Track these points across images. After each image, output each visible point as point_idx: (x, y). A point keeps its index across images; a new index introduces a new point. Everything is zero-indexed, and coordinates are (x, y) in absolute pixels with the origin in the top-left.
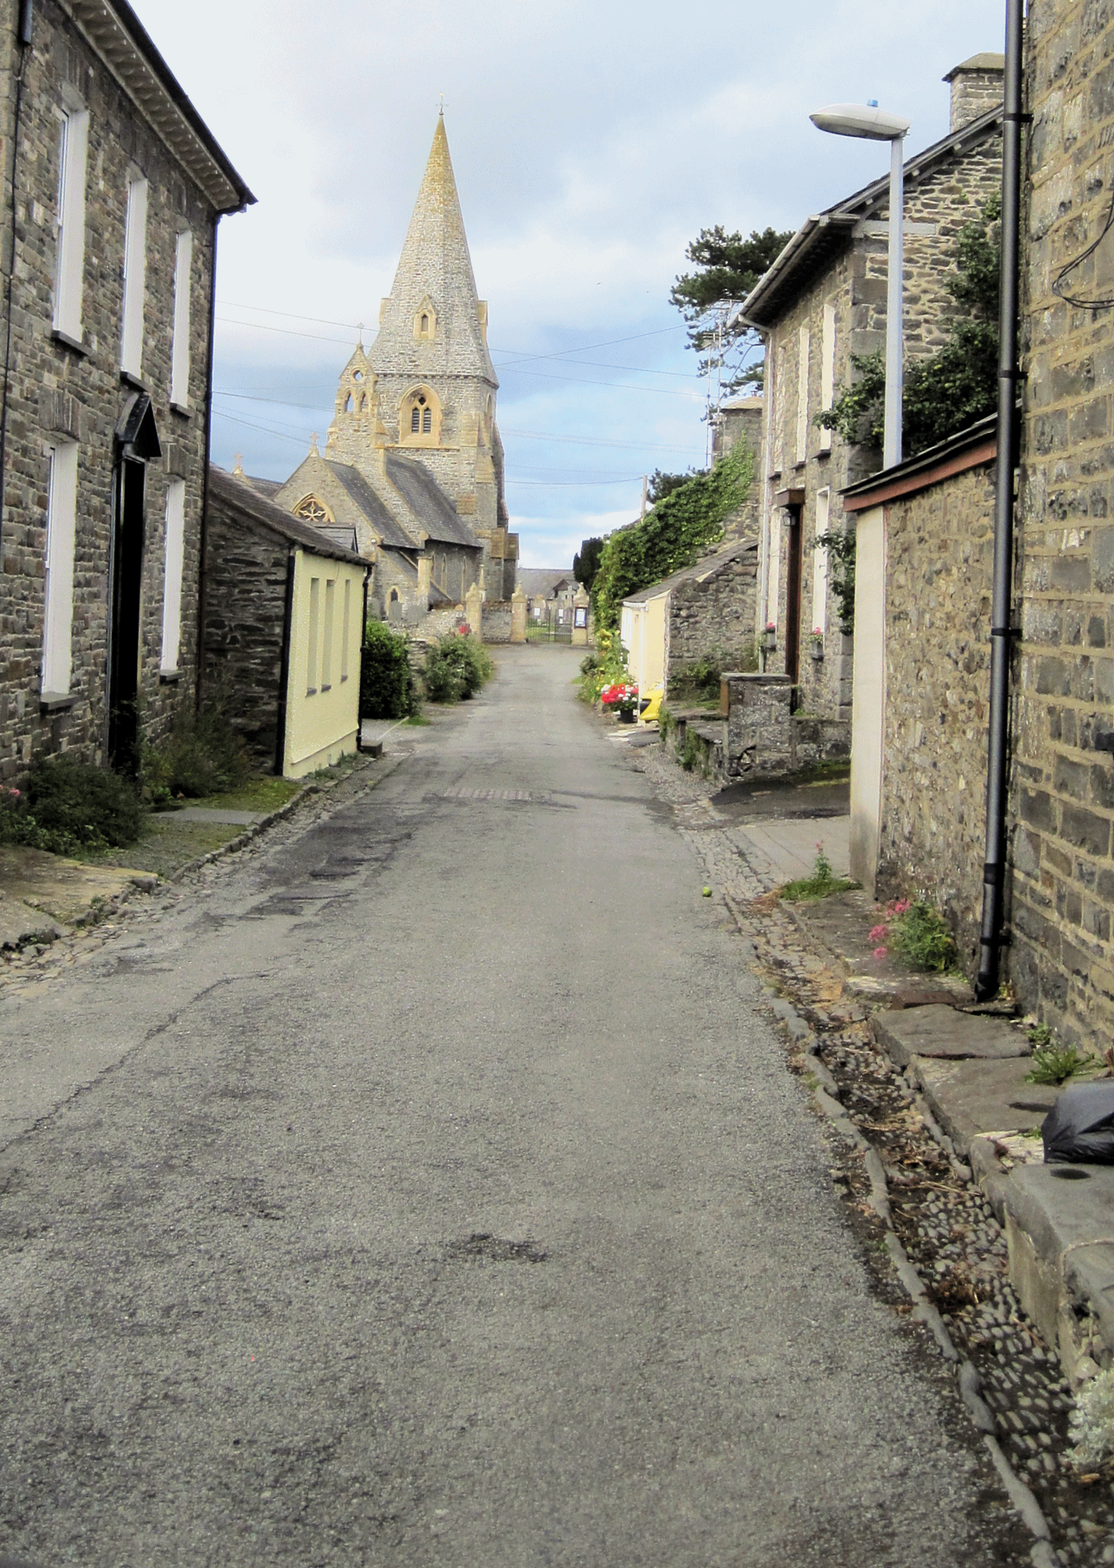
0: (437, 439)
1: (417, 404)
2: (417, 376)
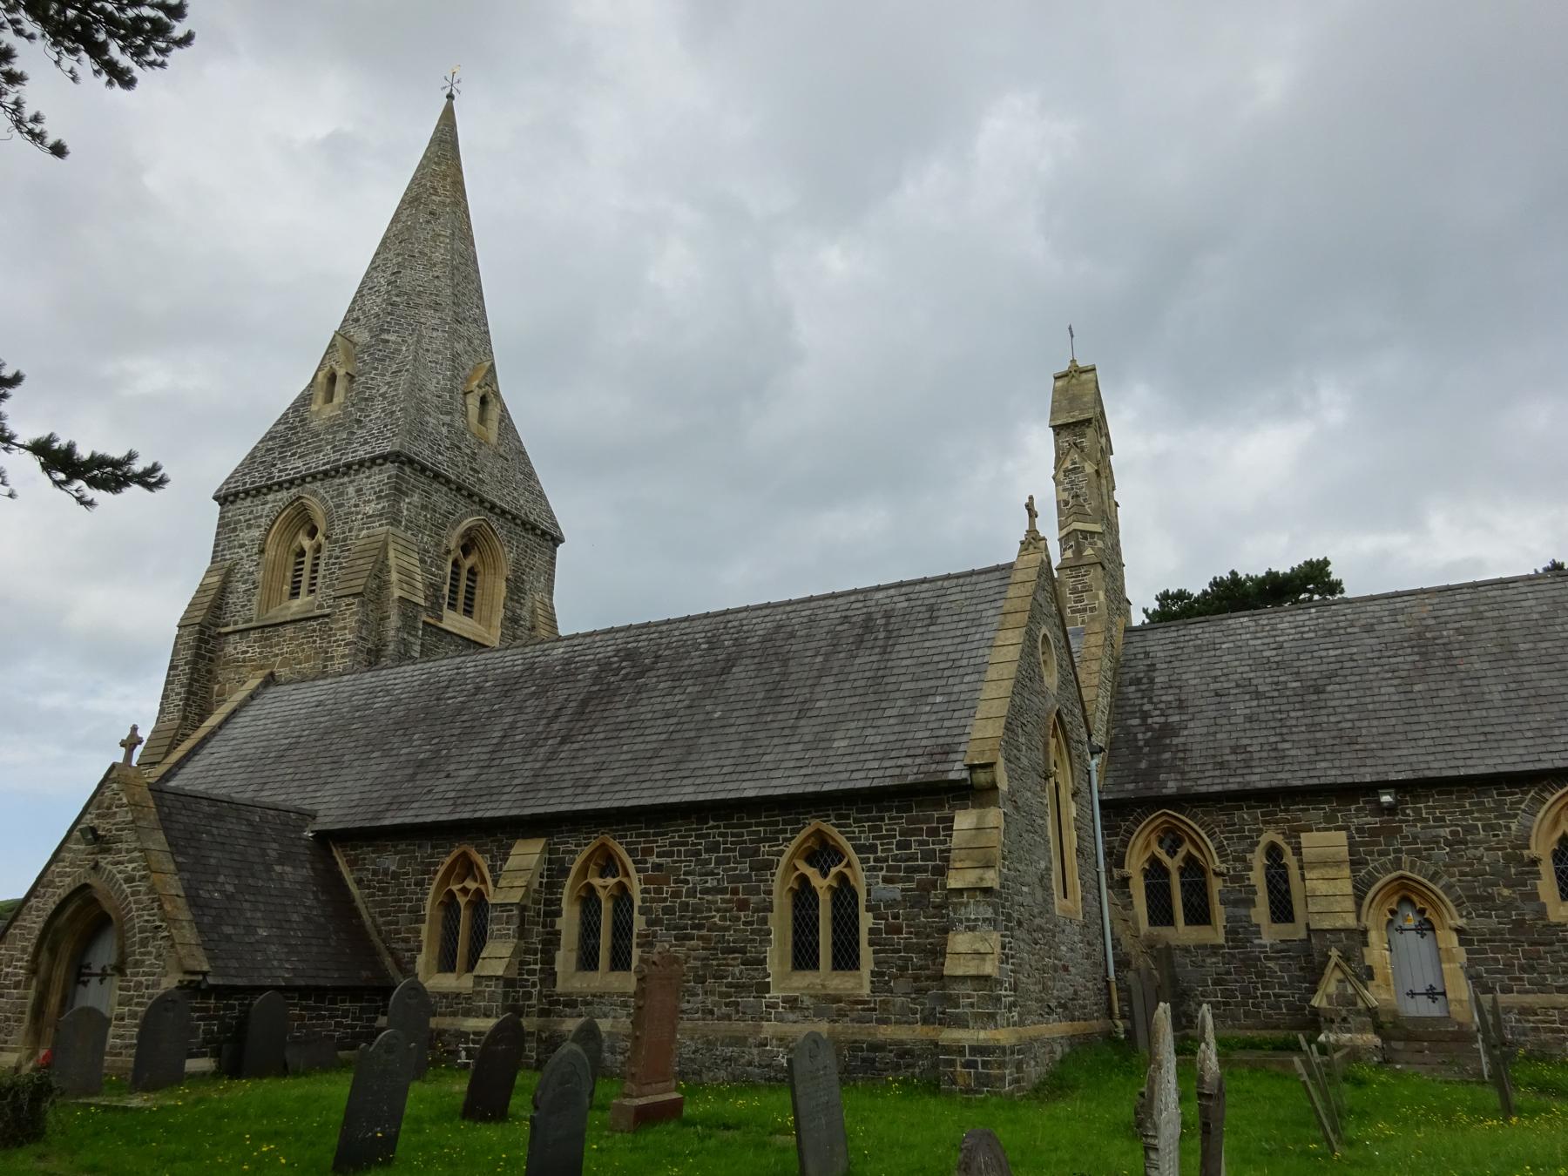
2: (482, 501)
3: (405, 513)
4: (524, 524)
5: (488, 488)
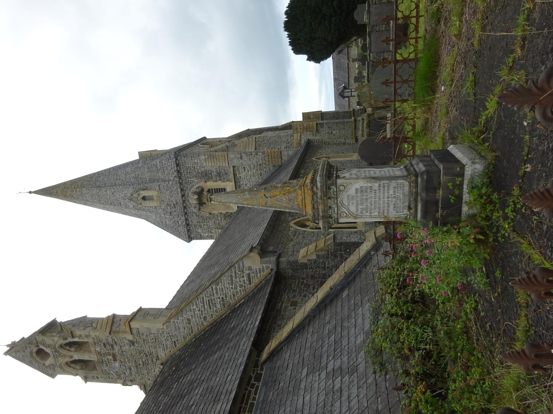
0: (228, 183)
2: (184, 202)
3: (207, 234)
5: (177, 199)
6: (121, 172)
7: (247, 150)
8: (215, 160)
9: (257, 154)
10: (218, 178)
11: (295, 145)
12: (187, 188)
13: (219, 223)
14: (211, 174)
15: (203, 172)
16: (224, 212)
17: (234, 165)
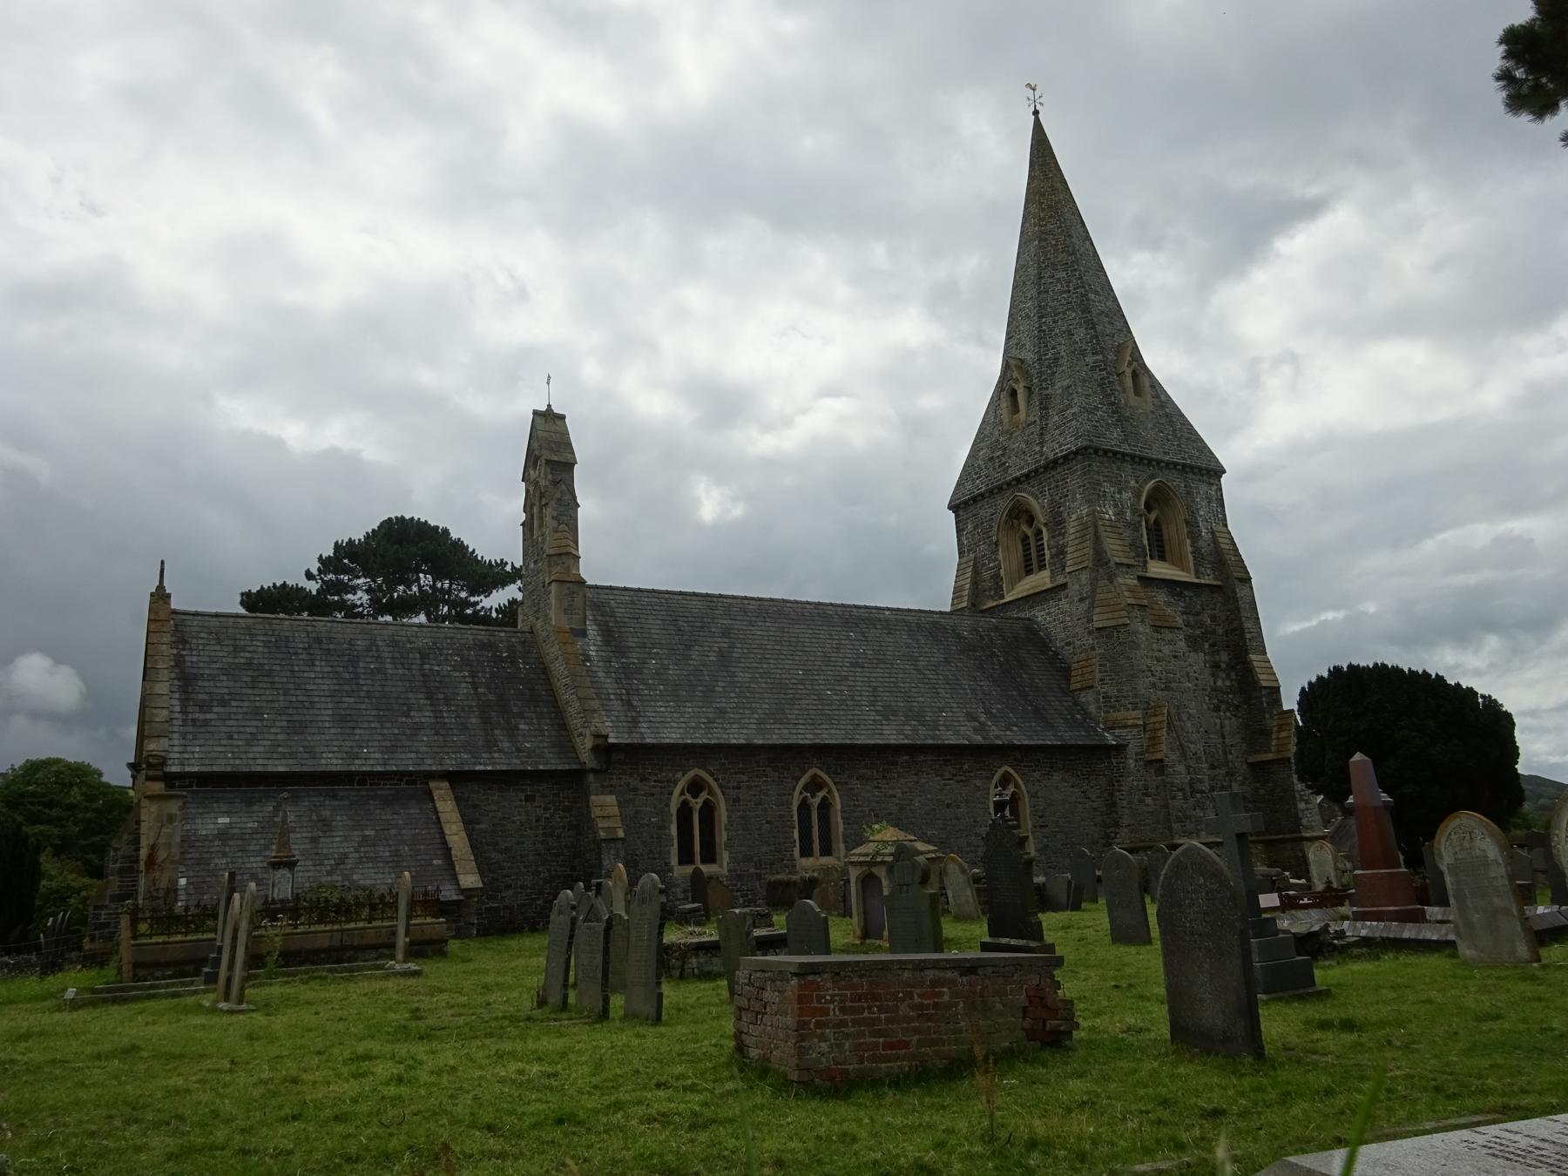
1: (1024, 528)
2: (1009, 484)
4: (1046, 467)
6: (1074, 318)
7: (1097, 610)
8: (1077, 542)
9: (1090, 633)
10: (1054, 550)
11: (1114, 715)
12: (1033, 487)
13: (985, 564)
14: (1059, 535)
15: (1061, 516)
16: (1002, 572)
17: (1070, 585)
